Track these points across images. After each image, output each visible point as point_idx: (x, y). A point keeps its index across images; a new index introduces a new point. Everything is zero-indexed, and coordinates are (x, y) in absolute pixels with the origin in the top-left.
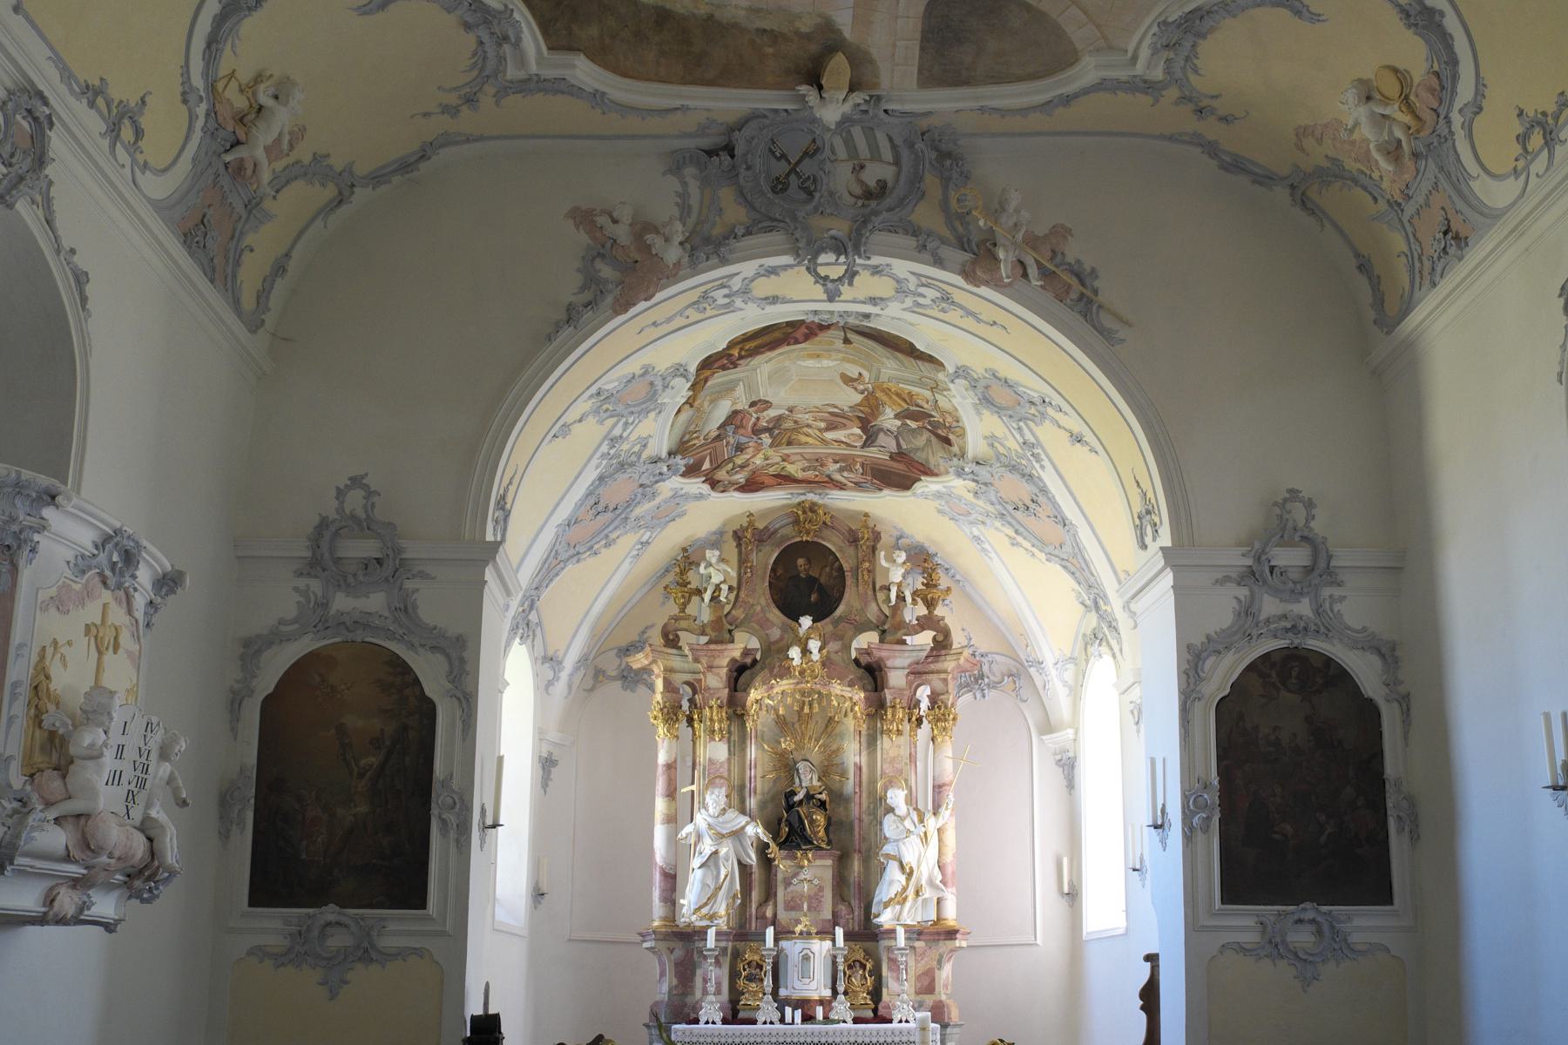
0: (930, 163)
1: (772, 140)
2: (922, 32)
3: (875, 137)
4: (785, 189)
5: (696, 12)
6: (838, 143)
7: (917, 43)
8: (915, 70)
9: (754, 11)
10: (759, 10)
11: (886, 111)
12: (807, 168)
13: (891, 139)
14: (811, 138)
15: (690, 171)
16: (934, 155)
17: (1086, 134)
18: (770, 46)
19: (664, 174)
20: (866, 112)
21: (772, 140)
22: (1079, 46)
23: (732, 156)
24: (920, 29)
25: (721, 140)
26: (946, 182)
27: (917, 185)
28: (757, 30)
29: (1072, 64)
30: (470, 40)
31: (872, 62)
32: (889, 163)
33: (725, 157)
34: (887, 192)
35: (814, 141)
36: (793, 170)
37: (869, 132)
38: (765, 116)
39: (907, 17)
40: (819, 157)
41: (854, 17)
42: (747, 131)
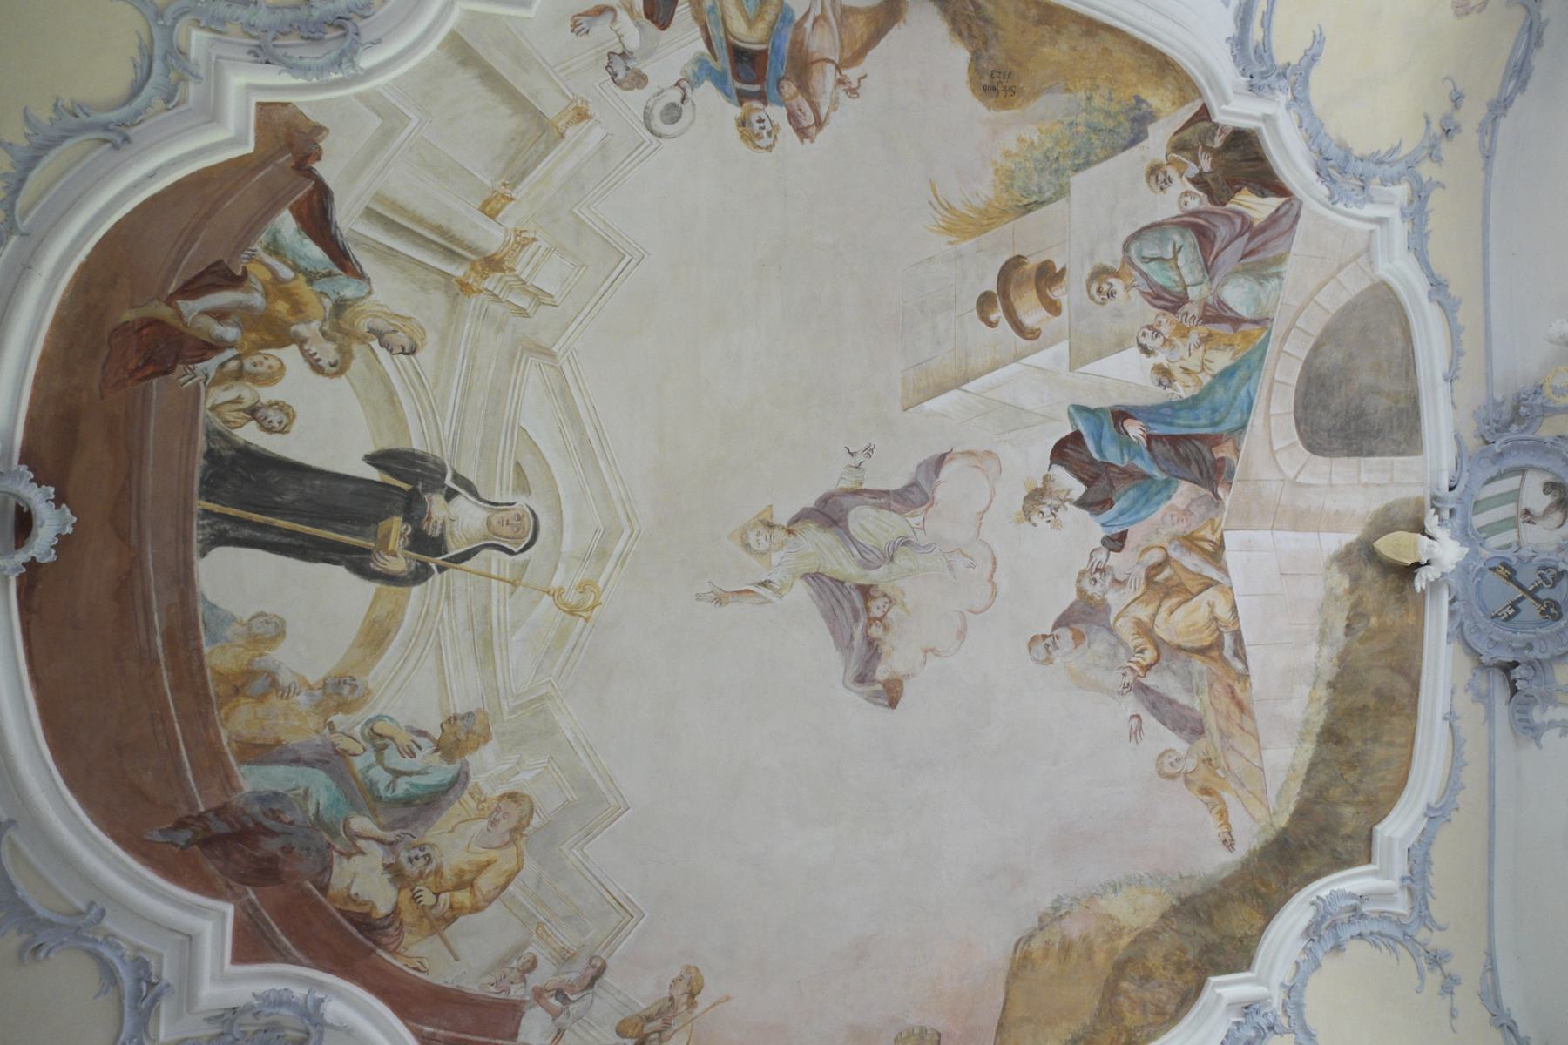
0: (1523, 431)
1: (1493, 617)
2: (1348, 456)
3: (1489, 498)
4: (1553, 603)
6: (1496, 541)
7: (1362, 459)
8: (1397, 460)
9: (1323, 637)
10: (1322, 632)
11: (1451, 489)
12: (1528, 577)
13: (1492, 480)
14: (1490, 574)
15: (1537, 716)
16: (1514, 428)
17: (1485, 255)
18: (1368, 620)
19: (1540, 746)
20: (1452, 512)
21: (1493, 617)
22: (1366, 284)
23: (1515, 664)
24: (1346, 459)
25: (1498, 677)
26: (1546, 411)
27: (1548, 445)
28: (1346, 634)
29: (1390, 289)
31: (1388, 509)
32: (1523, 480)
33: (1517, 673)
34: (1559, 481)
35: (1493, 569)
36: (1532, 594)
37: (1479, 506)
38: (1461, 625)
39: (1331, 474)
40: (1514, 562)
41: (1330, 531)
42: (1481, 647)
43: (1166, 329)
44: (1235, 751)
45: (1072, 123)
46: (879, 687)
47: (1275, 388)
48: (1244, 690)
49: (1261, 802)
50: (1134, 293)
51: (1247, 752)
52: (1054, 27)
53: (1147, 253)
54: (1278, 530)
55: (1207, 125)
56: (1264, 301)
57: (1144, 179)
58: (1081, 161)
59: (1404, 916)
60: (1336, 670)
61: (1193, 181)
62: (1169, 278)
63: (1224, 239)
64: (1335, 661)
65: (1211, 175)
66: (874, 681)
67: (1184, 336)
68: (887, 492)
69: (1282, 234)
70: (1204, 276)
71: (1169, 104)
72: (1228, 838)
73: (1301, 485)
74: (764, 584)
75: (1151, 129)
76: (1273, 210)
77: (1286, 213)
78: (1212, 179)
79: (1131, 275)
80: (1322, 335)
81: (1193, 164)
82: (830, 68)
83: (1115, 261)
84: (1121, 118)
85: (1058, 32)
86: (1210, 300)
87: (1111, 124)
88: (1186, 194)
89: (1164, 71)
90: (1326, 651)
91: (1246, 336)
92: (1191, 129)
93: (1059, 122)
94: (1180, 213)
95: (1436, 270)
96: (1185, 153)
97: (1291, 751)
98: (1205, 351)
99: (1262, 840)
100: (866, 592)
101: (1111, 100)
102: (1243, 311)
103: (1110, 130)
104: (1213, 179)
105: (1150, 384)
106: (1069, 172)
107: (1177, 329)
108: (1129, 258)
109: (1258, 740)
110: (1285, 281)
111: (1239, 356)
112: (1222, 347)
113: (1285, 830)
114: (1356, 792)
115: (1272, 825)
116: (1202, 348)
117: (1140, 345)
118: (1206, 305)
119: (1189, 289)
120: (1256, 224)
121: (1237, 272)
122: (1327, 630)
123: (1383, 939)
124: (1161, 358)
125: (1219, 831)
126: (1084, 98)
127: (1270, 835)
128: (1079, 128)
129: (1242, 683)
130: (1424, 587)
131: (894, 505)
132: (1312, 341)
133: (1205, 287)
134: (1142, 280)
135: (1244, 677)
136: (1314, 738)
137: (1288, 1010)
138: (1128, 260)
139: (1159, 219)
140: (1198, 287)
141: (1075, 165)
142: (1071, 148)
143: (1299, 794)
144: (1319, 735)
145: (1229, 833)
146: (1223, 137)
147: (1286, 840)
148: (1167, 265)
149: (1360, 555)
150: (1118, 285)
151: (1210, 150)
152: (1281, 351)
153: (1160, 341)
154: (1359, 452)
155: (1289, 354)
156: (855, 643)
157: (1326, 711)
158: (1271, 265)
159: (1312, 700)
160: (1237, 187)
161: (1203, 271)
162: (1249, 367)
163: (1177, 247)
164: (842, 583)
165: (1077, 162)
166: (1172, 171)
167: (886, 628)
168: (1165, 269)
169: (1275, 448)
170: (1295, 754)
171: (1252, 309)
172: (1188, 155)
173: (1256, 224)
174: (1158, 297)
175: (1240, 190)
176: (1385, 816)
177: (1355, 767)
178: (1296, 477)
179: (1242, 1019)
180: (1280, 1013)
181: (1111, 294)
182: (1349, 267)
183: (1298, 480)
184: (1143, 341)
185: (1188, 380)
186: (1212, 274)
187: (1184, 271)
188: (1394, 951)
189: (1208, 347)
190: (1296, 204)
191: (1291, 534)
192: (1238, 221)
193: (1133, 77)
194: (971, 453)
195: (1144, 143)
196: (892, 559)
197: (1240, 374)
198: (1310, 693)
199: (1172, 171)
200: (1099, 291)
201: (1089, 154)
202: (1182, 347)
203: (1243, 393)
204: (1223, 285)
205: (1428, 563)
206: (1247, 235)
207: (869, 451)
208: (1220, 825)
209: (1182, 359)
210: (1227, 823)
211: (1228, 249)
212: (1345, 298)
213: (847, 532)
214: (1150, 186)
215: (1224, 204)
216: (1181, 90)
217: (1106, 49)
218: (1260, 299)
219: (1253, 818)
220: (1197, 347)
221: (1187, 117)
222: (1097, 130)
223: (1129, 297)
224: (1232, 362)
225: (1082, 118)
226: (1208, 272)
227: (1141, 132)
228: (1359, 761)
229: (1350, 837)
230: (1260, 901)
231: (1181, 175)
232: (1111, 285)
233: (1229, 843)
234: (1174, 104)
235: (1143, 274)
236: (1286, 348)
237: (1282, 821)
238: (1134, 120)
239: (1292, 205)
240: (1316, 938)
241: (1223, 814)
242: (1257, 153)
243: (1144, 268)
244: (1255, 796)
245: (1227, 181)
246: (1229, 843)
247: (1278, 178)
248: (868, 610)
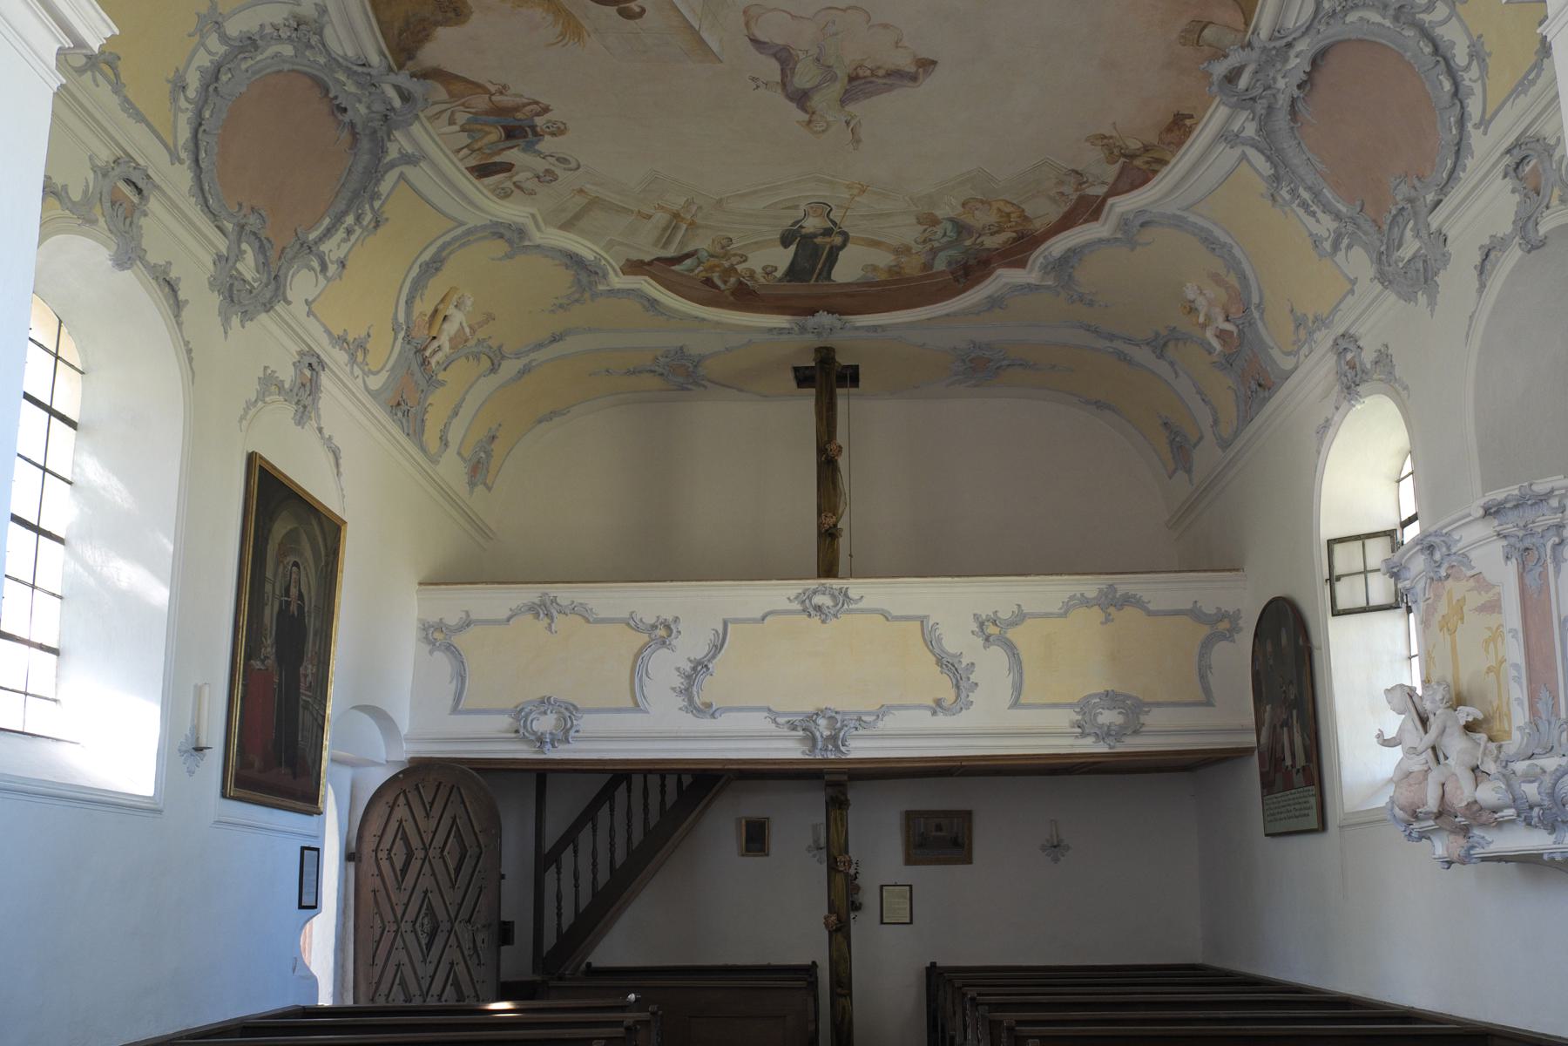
46: (921, 70)
66: (917, 72)
68: (782, 70)
74: (848, 123)
82: (494, 98)
100: (852, 79)
131: (791, 66)
156: (889, 82)
164: (846, 90)
167: (879, 68)
194: (747, 24)
196: (829, 67)
207: (753, 79)
213: (812, 88)
248: (865, 77)
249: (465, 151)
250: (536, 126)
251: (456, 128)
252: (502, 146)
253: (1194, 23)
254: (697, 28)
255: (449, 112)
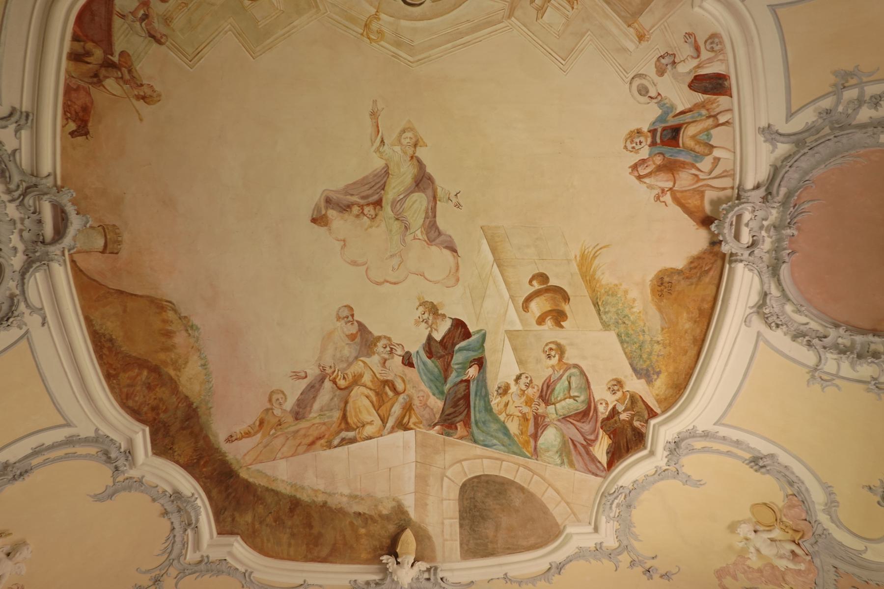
2: (459, 511)
5: (316, 499)
7: (457, 520)
8: (458, 543)
9: (353, 497)
10: (356, 497)
11: (442, 579)
18: (363, 527)
28: (354, 513)
30: (165, 524)
31: (429, 538)
39: (449, 500)
41: (416, 500)
43: (530, 391)
44: (286, 442)
45: (644, 332)
46: (323, 212)
47: (499, 462)
48: (322, 446)
49: (255, 460)
50: (550, 371)
51: (285, 449)
52: (698, 319)
53: (573, 379)
54: (416, 466)
55: (646, 417)
56: (547, 454)
57: (614, 377)
58: (623, 338)
59: (185, 559)
60: (334, 507)
61: (614, 408)
62: (559, 393)
63: (582, 428)
64: (339, 506)
65: (617, 420)
66: (327, 208)
67: (526, 403)
68: (435, 217)
69: (586, 465)
70: (560, 416)
71: (657, 392)
72: (234, 438)
73: (442, 480)
75: (643, 381)
76: (600, 460)
77: (597, 467)
78: (615, 420)
79: (560, 369)
80: (529, 492)
81: (623, 408)
82: (670, 184)
83: (568, 359)
84: (648, 362)
85: (695, 322)
86: (547, 420)
87: (645, 356)
88: (607, 404)
89: (676, 388)
90: (345, 500)
91: (528, 442)
92: (643, 407)
93: (645, 324)
94: (596, 400)
95: (567, 567)
96: (630, 403)
97: (285, 478)
98: (518, 417)
99: (234, 462)
100: (378, 203)
101: (658, 356)
102: (541, 441)
103: (641, 356)
104: (616, 422)
105: (499, 381)
106: (617, 330)
107: (530, 398)
108: (570, 368)
109: (291, 456)
110: (559, 467)
111: (516, 439)
112: (521, 427)
113: (238, 476)
114: (261, 523)
115: (241, 467)
116: (520, 415)
117: (521, 375)
118: (545, 417)
119: (553, 406)
120: (591, 448)
121: (564, 437)
122: (357, 500)
123: (171, 545)
124: (513, 388)
125: (238, 432)
126: (659, 339)
127: (235, 466)
128: (642, 336)
129: (325, 444)
130: (383, 562)
131: (428, 221)
132: (525, 486)
133: (554, 416)
134: (557, 375)
135: (329, 445)
136: (293, 493)
137: (127, 481)
138: (568, 367)
139: (592, 387)
140: (554, 412)
141: (621, 334)
142: (631, 332)
143: (260, 484)
144: (295, 496)
145: (236, 439)
146: (640, 426)
147: (232, 477)
148: (566, 392)
149: (401, 520)
150: (554, 361)
151: (632, 419)
152: (519, 465)
153: (524, 388)
154: (462, 518)
155: (517, 471)
156: (349, 197)
157: (309, 501)
158: (568, 458)
159: (316, 491)
160: (612, 436)
161: (564, 415)
162: (510, 445)
163: (577, 399)
164: (383, 189)
165: (623, 335)
166: (619, 394)
167: (357, 216)
168: (564, 391)
169: (463, 463)
170: (283, 481)
171: (542, 447)
172: (629, 405)
173: (591, 448)
174: (548, 387)
175: (610, 438)
176: (245, 542)
177: (275, 521)
178: (447, 477)
179: (122, 450)
180: (126, 475)
181: (549, 357)
182: (568, 509)
183: (445, 478)
184: (523, 377)
185: (502, 406)
186: (562, 420)
187: (563, 403)
188: (164, 552)
189: (521, 418)
190: (603, 474)
191: (413, 474)
192: (592, 437)
193: (671, 369)
195: (635, 377)
196: (397, 219)
197: (506, 439)
198: (320, 490)
199: (619, 394)
200: (551, 349)
201: (628, 343)
202: (520, 401)
203: (495, 441)
204: (555, 428)
205: (398, 563)
206: (585, 443)
207: (458, 205)
208: (241, 433)
209: (514, 402)
210: (243, 437)
211: (576, 431)
212: (551, 507)
213: (412, 192)
214: (611, 381)
215: (602, 429)
216: (665, 399)
217: (687, 352)
218: (548, 451)
219: (245, 455)
220: (520, 412)
221: (650, 404)
222: (641, 347)
223: (547, 368)
224: (512, 434)
225: (647, 338)
226: (563, 418)
227: (641, 374)
228: (279, 524)
229: (233, 520)
230: (195, 461)
231: (617, 401)
232: (554, 357)
233: (230, 439)
234: (657, 395)
235: (561, 376)
236: (521, 469)
237: (244, 474)
238: (647, 370)
239: (603, 471)
240: (172, 498)
241: (248, 434)
242: (631, 448)
243: (565, 377)
244: (258, 456)
245: (615, 430)
246: (230, 439)
247: (618, 461)
248: (368, 205)
249: (722, 119)
250: (650, 146)
251: (717, 153)
252: (688, 117)
253: (116, 251)
254: (495, 264)
255: (713, 175)
